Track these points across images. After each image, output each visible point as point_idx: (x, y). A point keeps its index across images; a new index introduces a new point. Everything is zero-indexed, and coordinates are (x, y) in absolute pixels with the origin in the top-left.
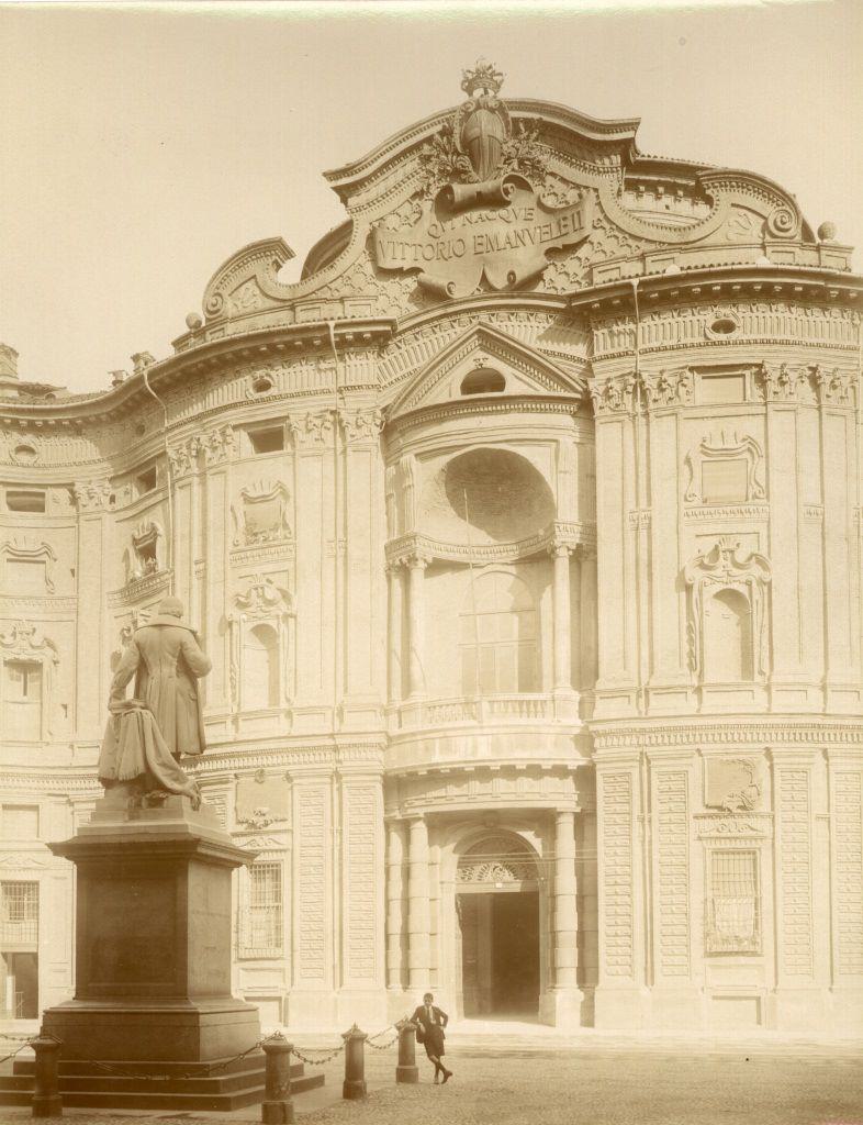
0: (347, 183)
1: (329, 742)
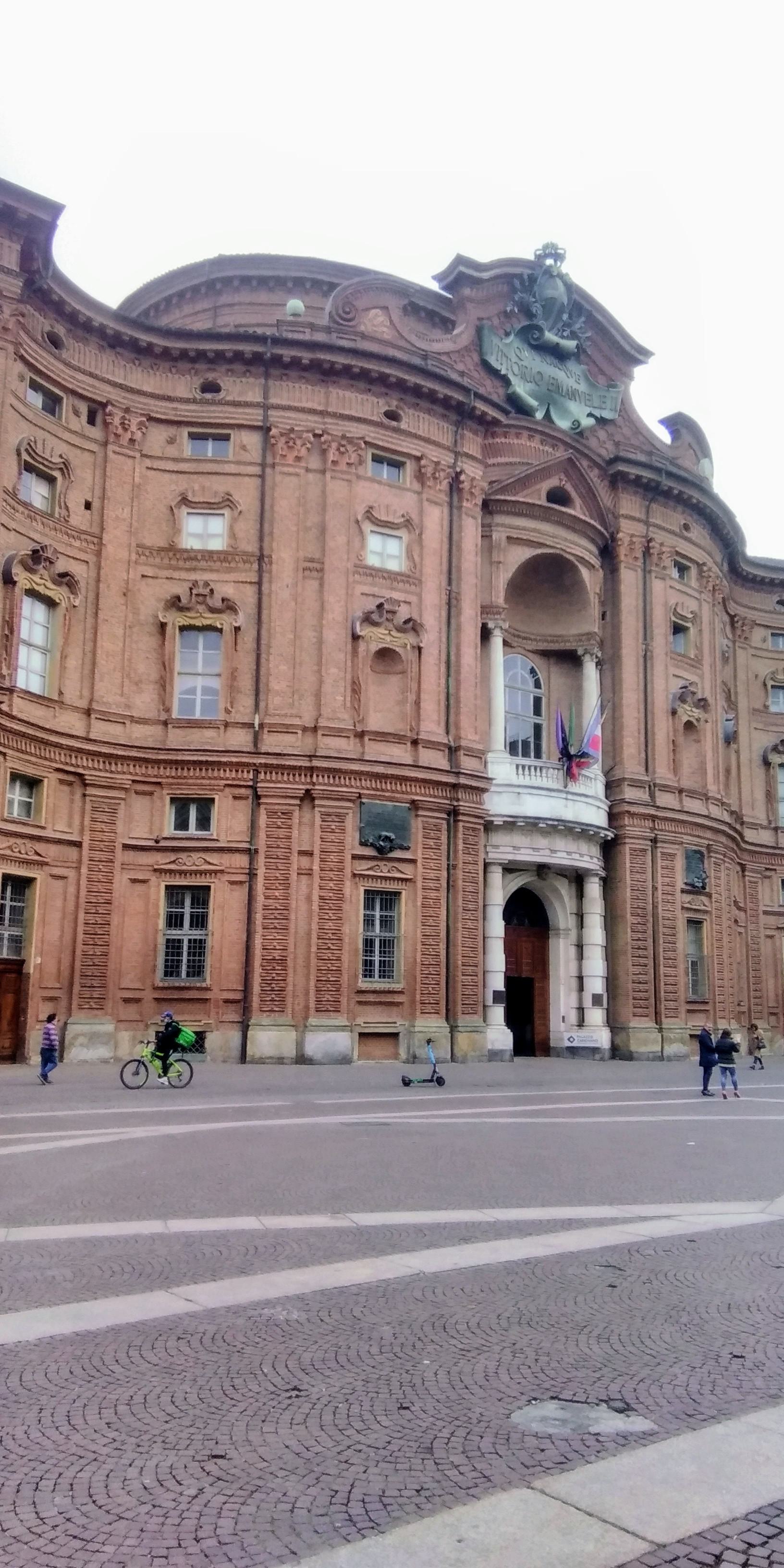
1: (451, 779)
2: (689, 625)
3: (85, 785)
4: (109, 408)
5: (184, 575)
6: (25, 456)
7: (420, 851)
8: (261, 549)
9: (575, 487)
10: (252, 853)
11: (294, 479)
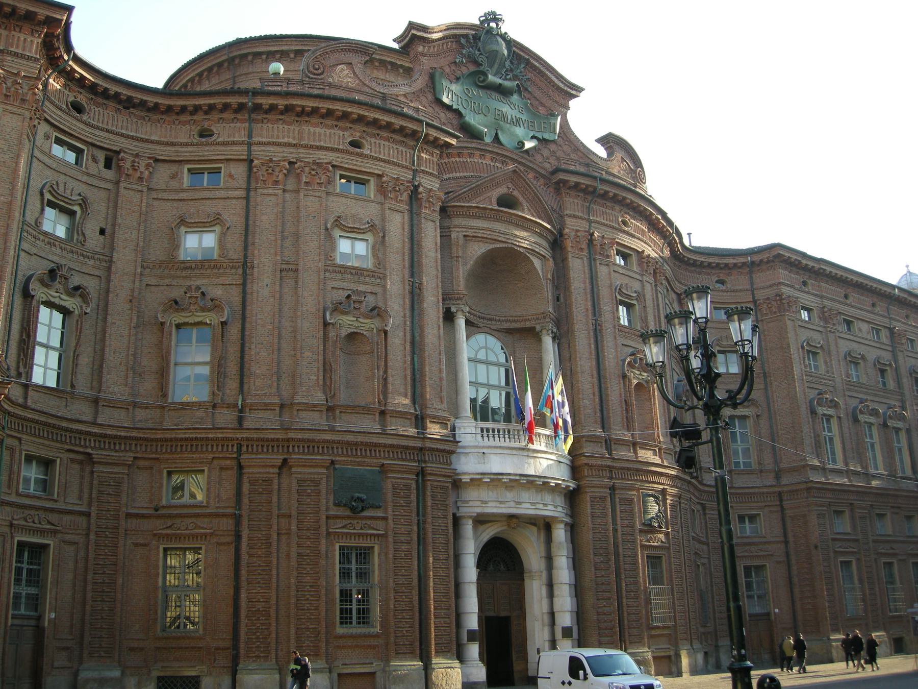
1: (419, 444)
2: (634, 302)
3: (94, 463)
4: (122, 154)
5: (181, 282)
6: (48, 196)
7: (390, 510)
8: (245, 256)
9: (523, 194)
10: (238, 519)
11: (273, 198)
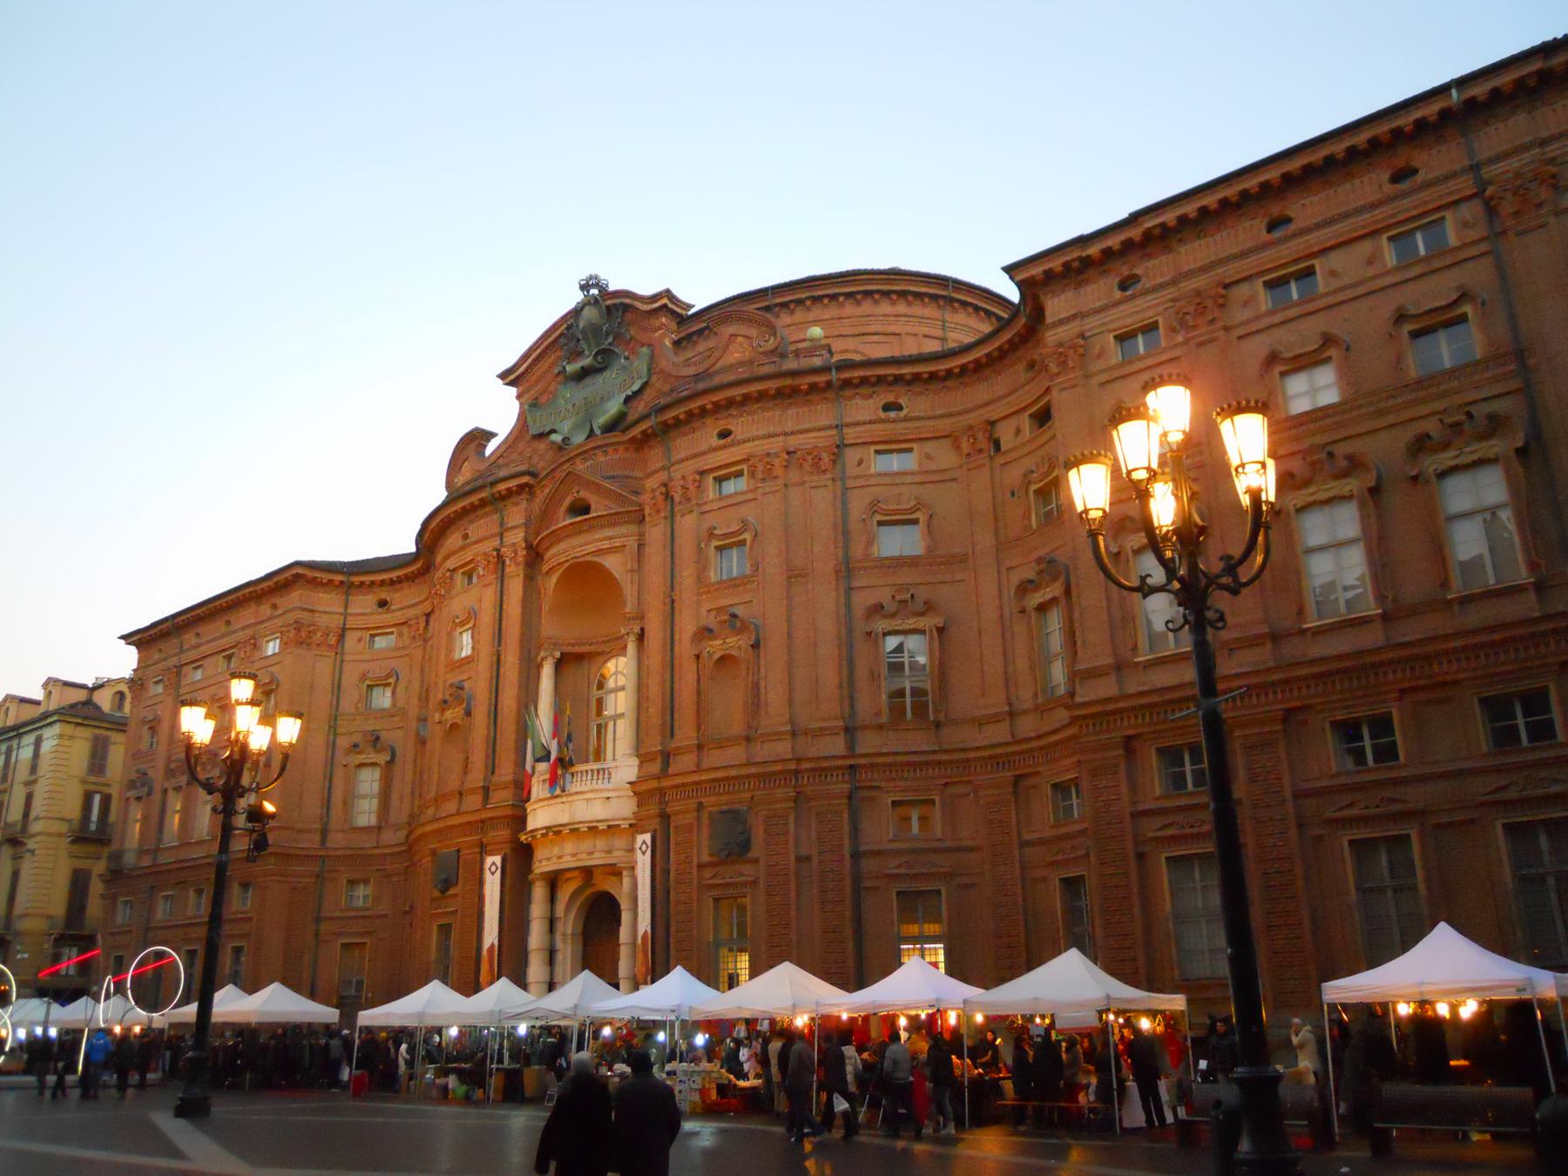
0: (510, 377)
